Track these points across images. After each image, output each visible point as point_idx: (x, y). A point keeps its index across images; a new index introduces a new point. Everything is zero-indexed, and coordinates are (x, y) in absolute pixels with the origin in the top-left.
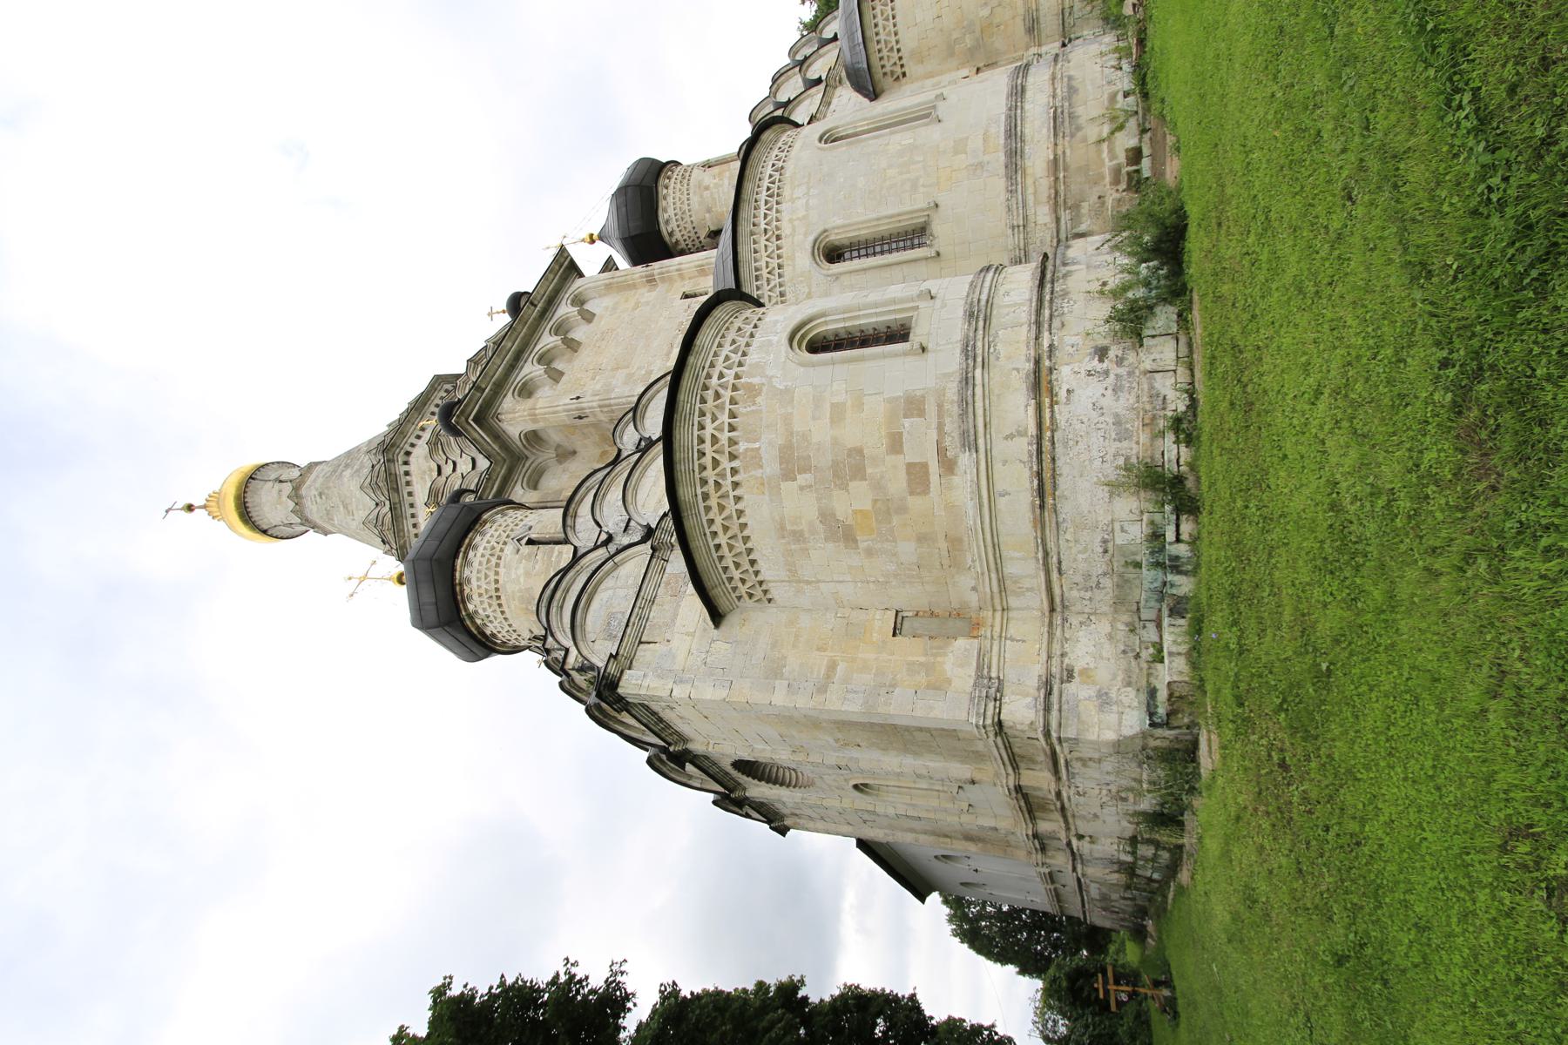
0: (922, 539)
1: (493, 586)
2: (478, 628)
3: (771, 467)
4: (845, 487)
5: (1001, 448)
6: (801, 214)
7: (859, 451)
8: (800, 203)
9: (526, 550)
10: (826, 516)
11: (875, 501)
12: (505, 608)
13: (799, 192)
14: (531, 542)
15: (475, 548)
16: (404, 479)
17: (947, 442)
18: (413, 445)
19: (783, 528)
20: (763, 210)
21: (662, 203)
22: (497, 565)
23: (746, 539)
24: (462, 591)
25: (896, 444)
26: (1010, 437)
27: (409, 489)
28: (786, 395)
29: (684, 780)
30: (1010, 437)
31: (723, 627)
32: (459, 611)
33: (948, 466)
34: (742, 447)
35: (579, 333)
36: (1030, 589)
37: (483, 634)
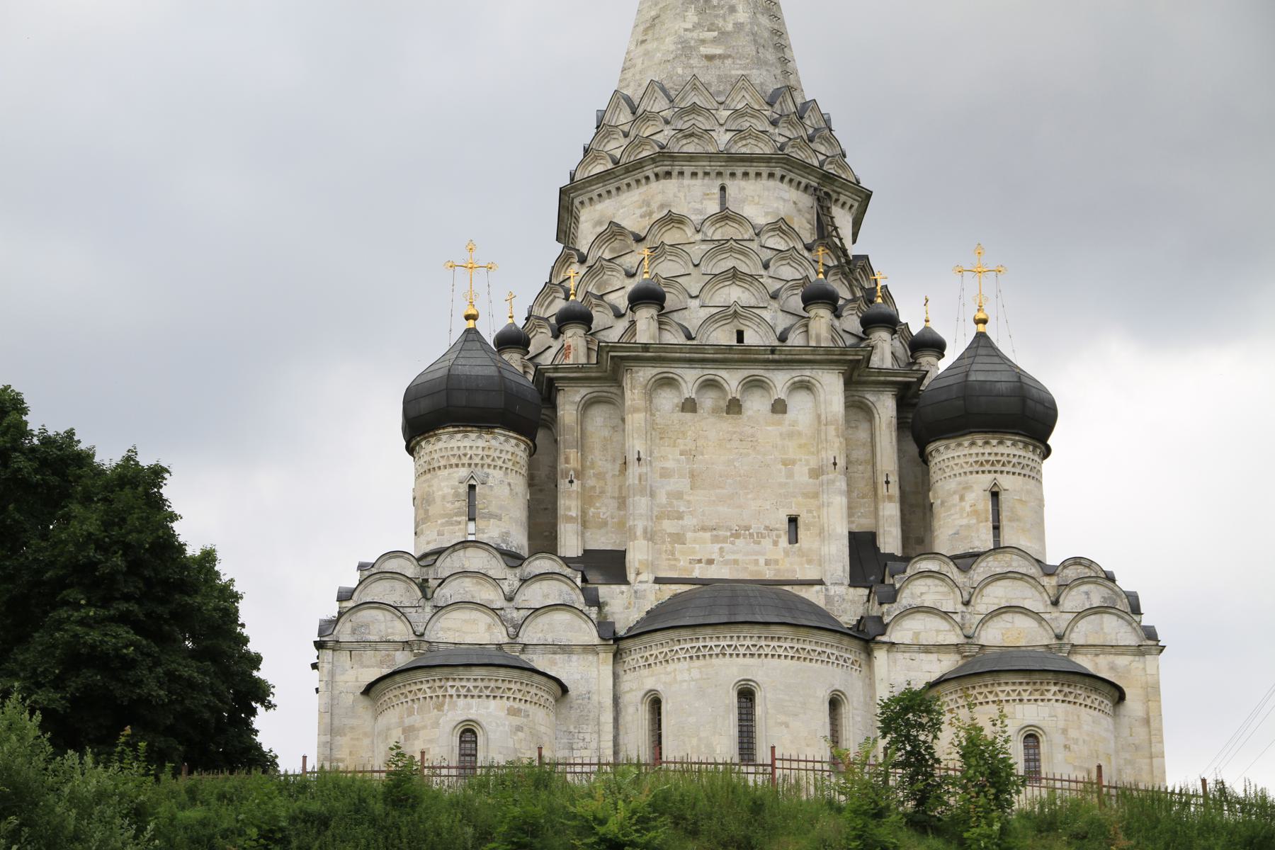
1: (436, 465)
3: (408, 721)
6: (679, 678)
8: (686, 676)
9: (463, 489)
13: (695, 673)
14: (472, 487)
15: (466, 437)
16: (640, 176)
18: (681, 173)
20: (688, 646)
21: (953, 443)
22: (451, 466)
27: (633, 184)
28: (436, 724)
31: (361, 698)
35: (756, 405)
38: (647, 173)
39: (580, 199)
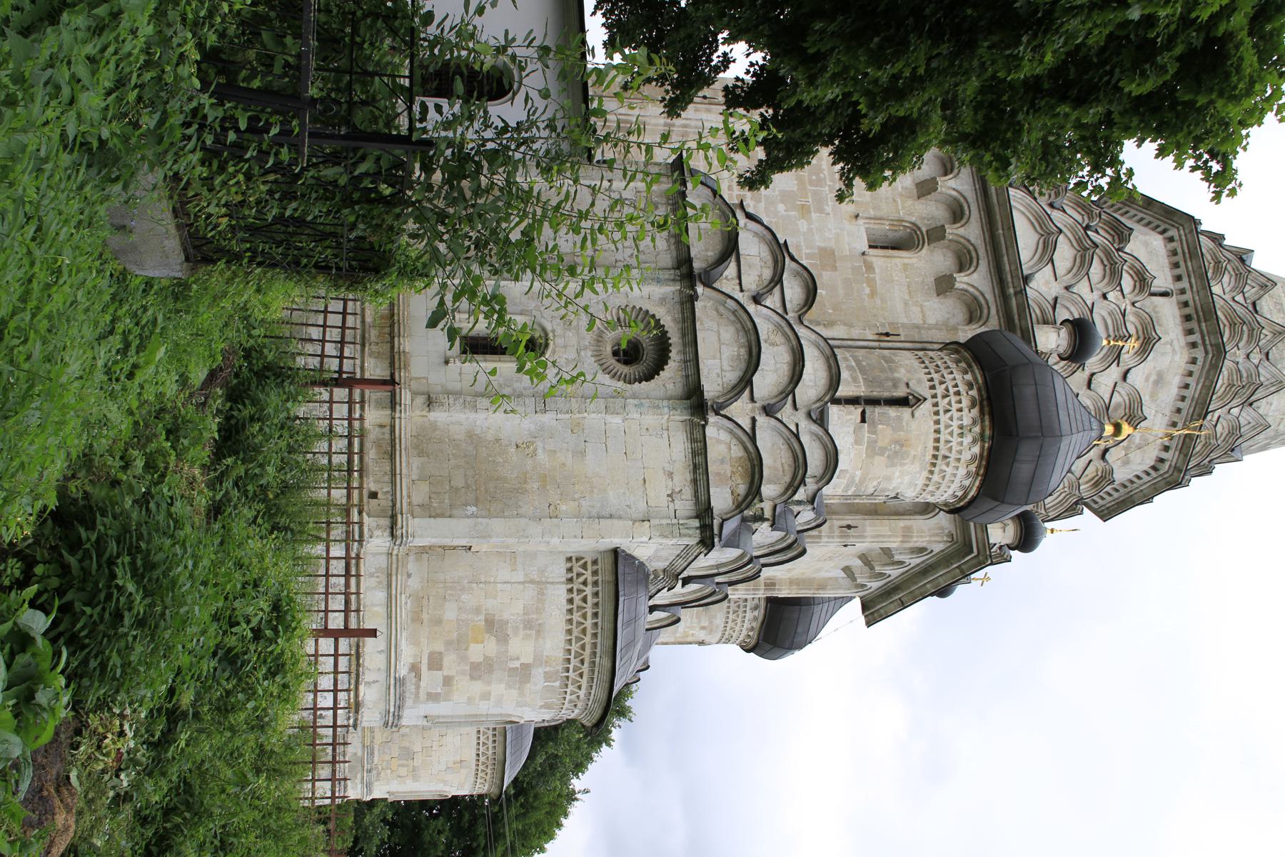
0: (438, 622)
1: (936, 470)
2: (983, 421)
3: (538, 673)
4: (486, 658)
5: (381, 677)
7: (472, 678)
10: (503, 639)
11: (466, 649)
12: (931, 444)
17: (414, 681)
19: (538, 632)
21: (756, 625)
23: (570, 621)
24: (978, 467)
25: (448, 681)
26: (374, 682)
29: (741, 312)
30: (374, 682)
32: (990, 449)
33: (415, 669)
34: (557, 684)
36: (372, 575)
37: (982, 412)
38: (1171, 452)
39: (1200, 362)
